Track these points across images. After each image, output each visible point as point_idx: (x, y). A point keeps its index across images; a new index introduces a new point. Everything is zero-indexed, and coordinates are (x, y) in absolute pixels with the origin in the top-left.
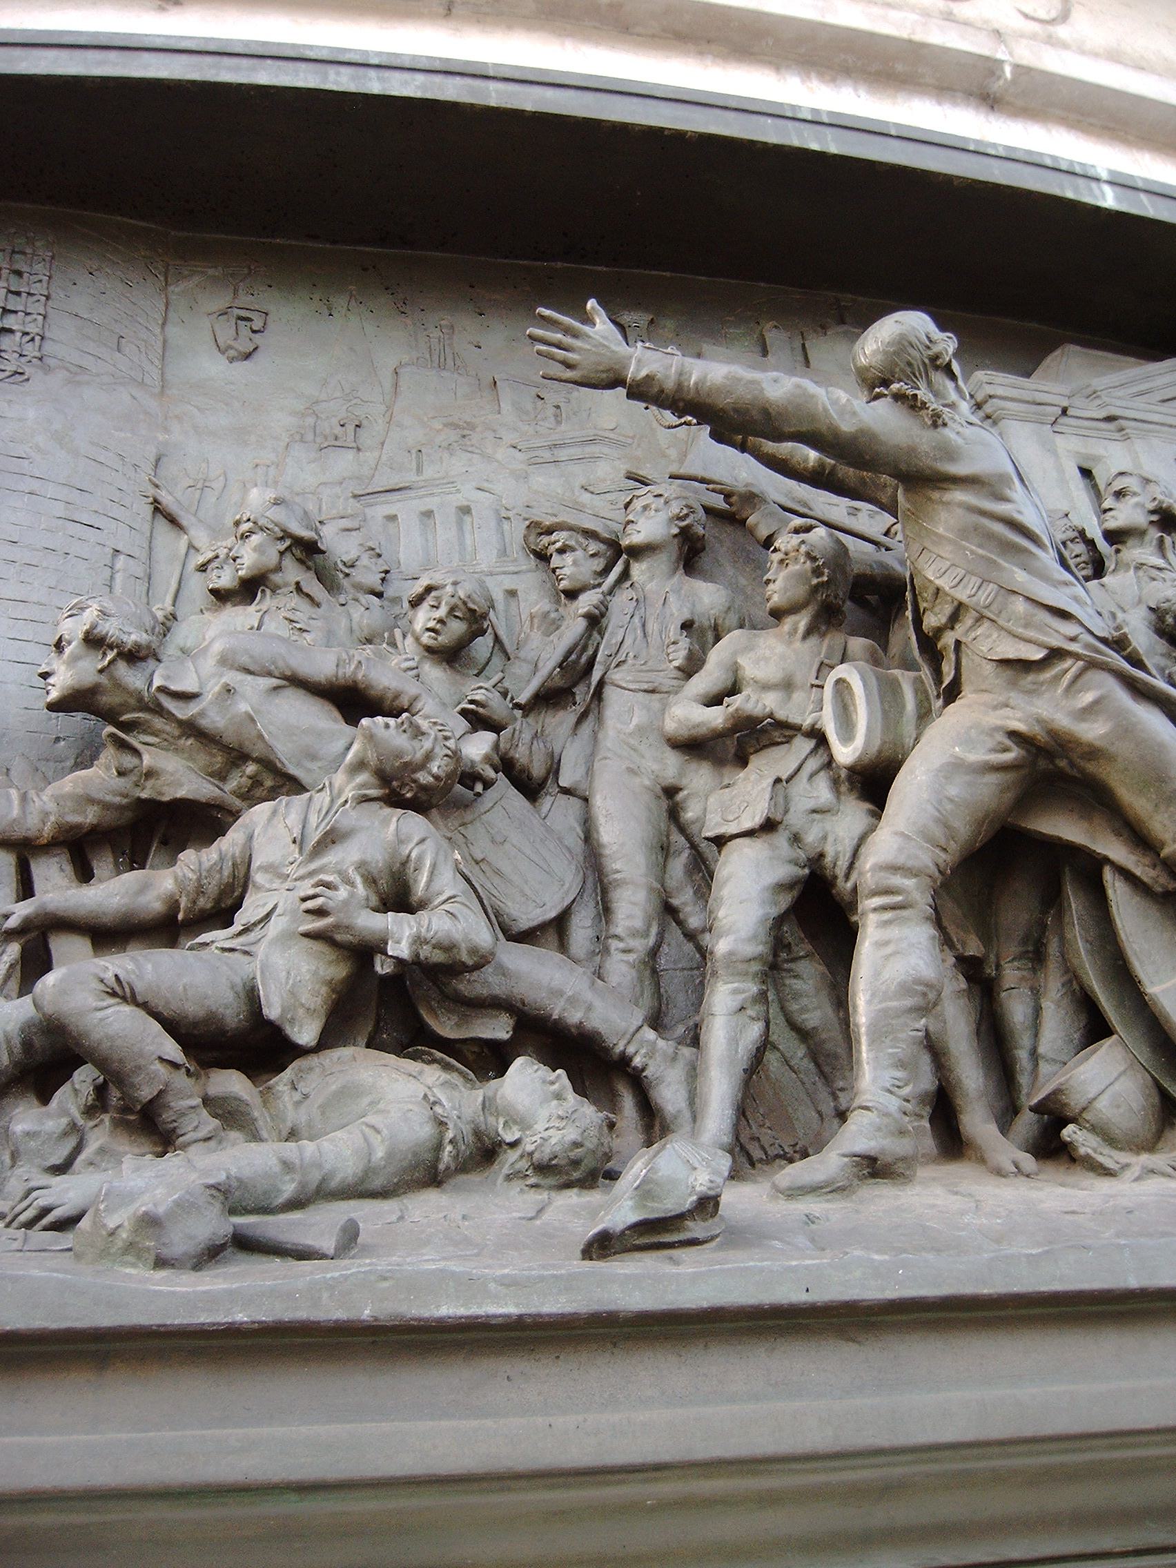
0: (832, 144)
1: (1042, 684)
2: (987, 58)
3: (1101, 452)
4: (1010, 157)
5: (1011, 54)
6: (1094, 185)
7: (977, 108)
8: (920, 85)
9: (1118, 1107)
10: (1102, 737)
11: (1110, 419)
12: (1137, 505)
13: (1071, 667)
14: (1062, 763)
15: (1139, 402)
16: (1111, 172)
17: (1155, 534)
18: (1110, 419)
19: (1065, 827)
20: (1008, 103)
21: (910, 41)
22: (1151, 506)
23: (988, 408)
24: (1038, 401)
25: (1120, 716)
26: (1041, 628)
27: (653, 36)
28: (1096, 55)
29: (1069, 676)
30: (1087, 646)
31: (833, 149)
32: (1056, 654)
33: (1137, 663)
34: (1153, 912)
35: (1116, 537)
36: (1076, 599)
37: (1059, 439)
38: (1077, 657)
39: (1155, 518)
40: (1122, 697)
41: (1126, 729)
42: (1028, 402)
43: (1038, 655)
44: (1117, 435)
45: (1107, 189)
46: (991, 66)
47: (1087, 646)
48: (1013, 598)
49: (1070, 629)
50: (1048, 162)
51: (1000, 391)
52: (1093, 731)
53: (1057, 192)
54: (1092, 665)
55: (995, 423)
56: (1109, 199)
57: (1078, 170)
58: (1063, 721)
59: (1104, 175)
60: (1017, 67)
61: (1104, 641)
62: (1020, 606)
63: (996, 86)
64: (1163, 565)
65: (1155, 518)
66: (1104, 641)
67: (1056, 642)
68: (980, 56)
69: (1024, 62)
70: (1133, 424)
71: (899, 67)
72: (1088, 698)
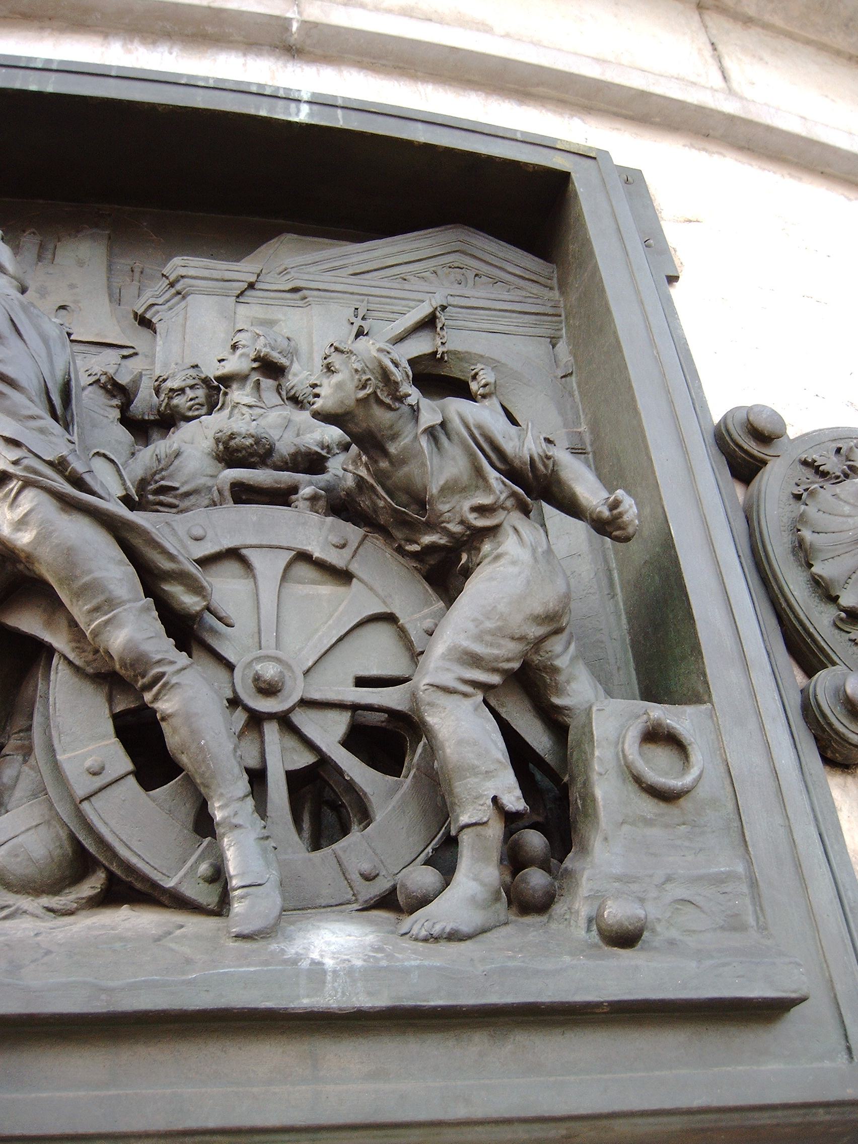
0: (51, 85)
2: (278, 17)
3: (280, 316)
4: (219, 87)
5: (300, 13)
6: (293, 105)
7: (278, 59)
8: (231, 42)
9: (17, 856)
11: (295, 290)
12: (242, 355)
13: (15, 485)
14: (21, 567)
15: (327, 277)
16: (313, 94)
17: (255, 377)
18: (295, 290)
19: (28, 622)
20: (309, 53)
21: (210, 8)
22: (252, 356)
23: (179, 287)
24: (227, 278)
27: (5, 17)
28: (389, 11)
31: (50, 89)
33: (78, 482)
34: (89, 689)
35: (226, 380)
36: (42, 431)
37: (242, 310)
38: (18, 478)
39: (255, 365)
40: (49, 508)
42: (217, 280)
44: (300, 303)
45: (305, 109)
46: (285, 23)
47: (28, 469)
50: (254, 89)
51: (192, 272)
52: (24, 539)
53: (252, 112)
54: (27, 484)
55: (184, 298)
56: (303, 115)
57: (281, 94)
59: (306, 97)
60: (304, 22)
61: (50, 464)
63: (292, 40)
64: (253, 403)
65: (255, 365)
66: (50, 464)
68: (271, 16)
69: (312, 19)
70: (315, 293)
71: (210, 29)
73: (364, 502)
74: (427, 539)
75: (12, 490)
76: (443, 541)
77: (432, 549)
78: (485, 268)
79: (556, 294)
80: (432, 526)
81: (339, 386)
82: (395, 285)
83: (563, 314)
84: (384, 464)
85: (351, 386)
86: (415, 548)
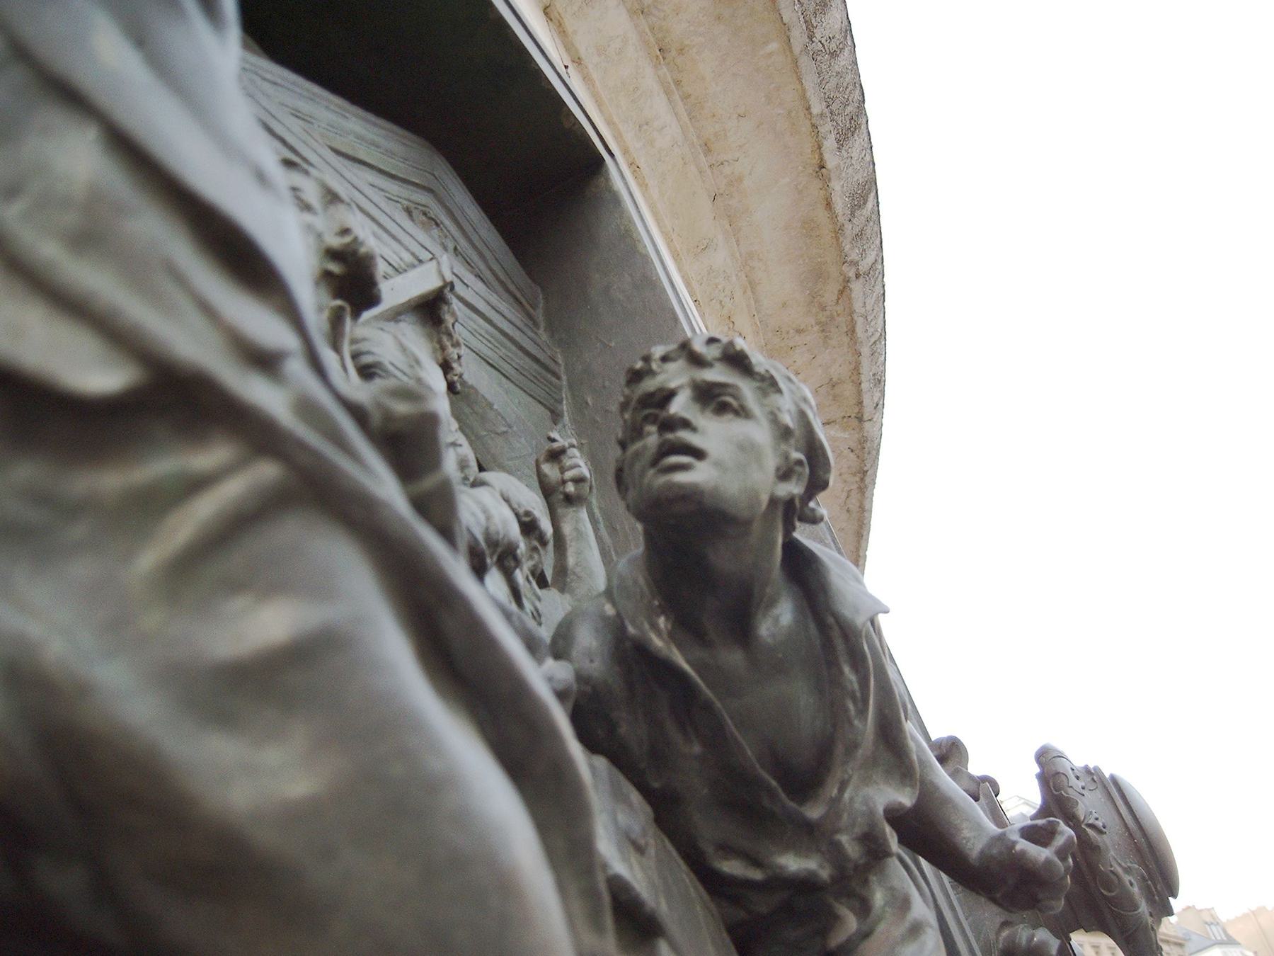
1: (74, 510)
10: (296, 816)
13: (230, 480)
14: (63, 882)
22: (336, 242)
25: (371, 733)
26: (138, 269)
29: (204, 509)
30: (307, 409)
32: (175, 400)
38: (258, 434)
41: (399, 801)
43: (97, 374)
47: (307, 409)
48: (54, 117)
49: (265, 326)
52: (255, 777)
54: (317, 491)
58: (126, 695)
62: (77, 157)
65: (335, 268)
67: (192, 345)
72: (267, 624)
73: (630, 729)
74: (793, 863)
75: (196, 485)
76: (825, 874)
77: (805, 885)
78: (463, 243)
79: (544, 336)
80: (811, 835)
81: (747, 448)
82: (383, 204)
83: (564, 377)
84: (733, 658)
85: (771, 463)
86: (732, 867)
